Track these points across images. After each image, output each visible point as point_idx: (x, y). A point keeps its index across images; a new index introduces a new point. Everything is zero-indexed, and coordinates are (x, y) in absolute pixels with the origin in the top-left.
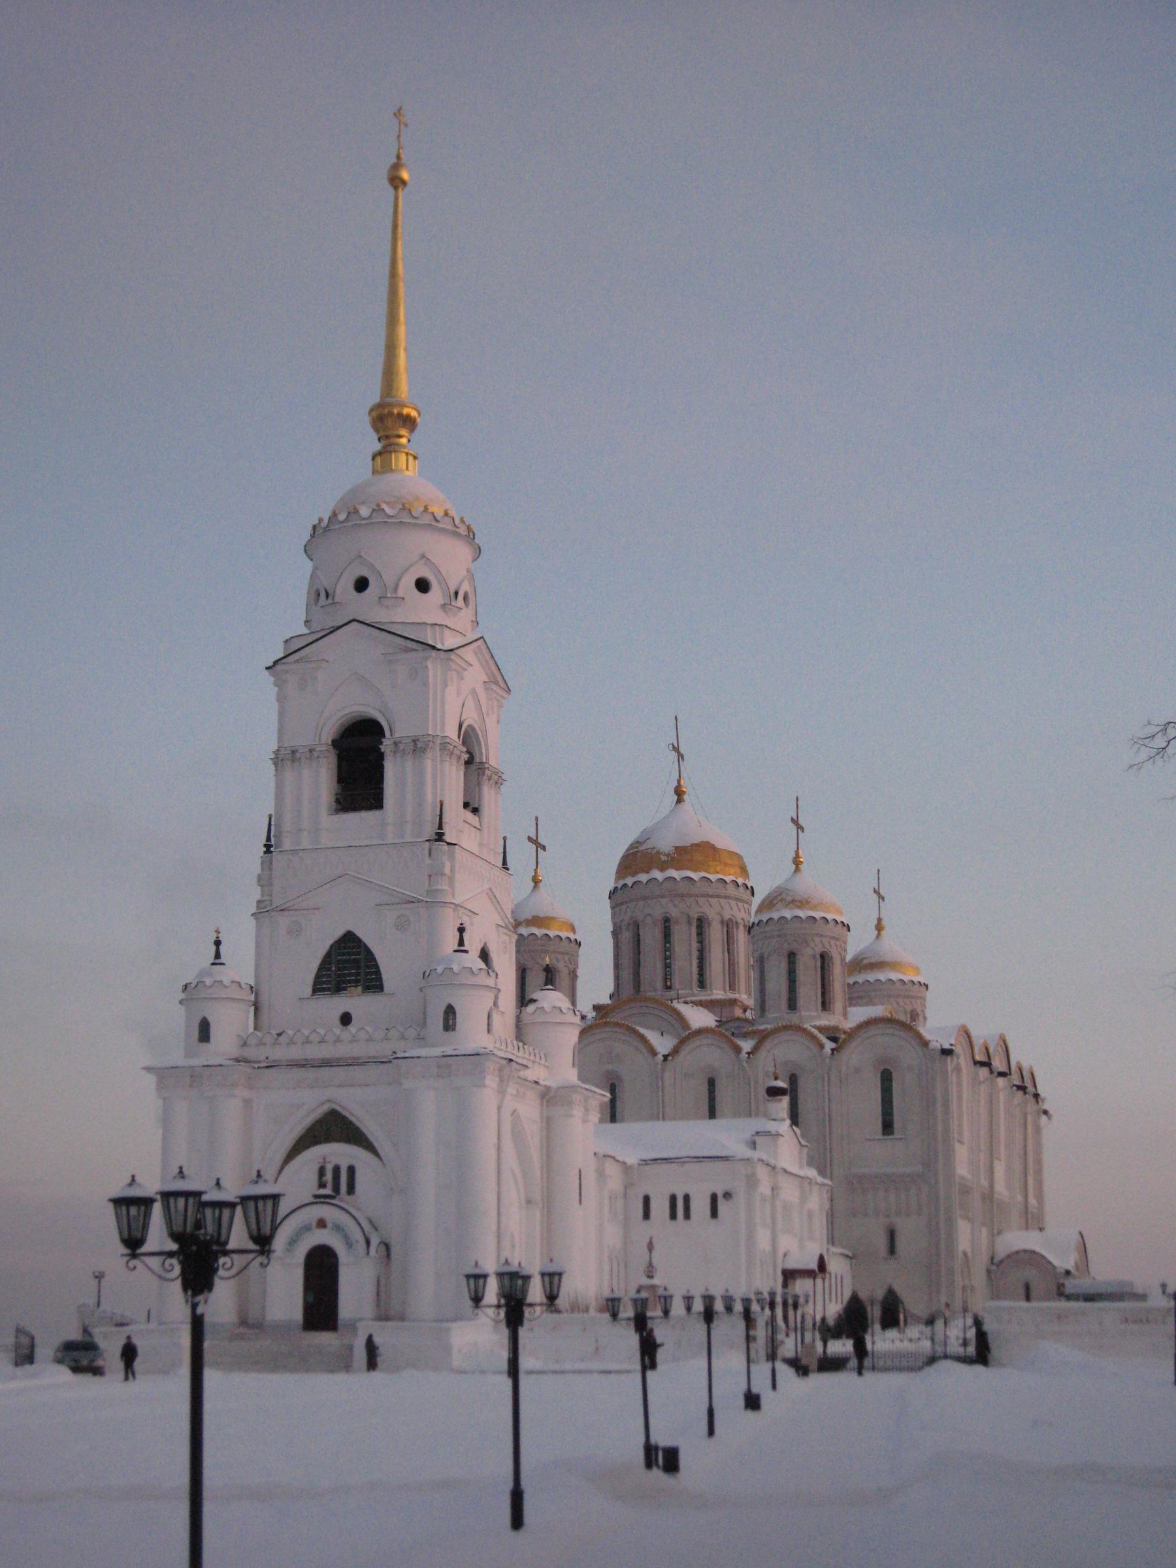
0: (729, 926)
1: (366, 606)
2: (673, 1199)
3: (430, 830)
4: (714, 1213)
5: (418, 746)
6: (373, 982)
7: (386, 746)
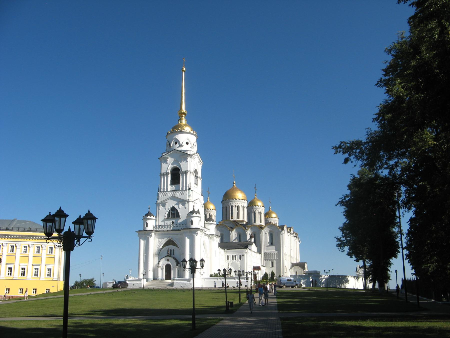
0: (243, 207)
2: (233, 256)
4: (240, 259)
5: (186, 172)
6: (178, 216)
7: (180, 172)
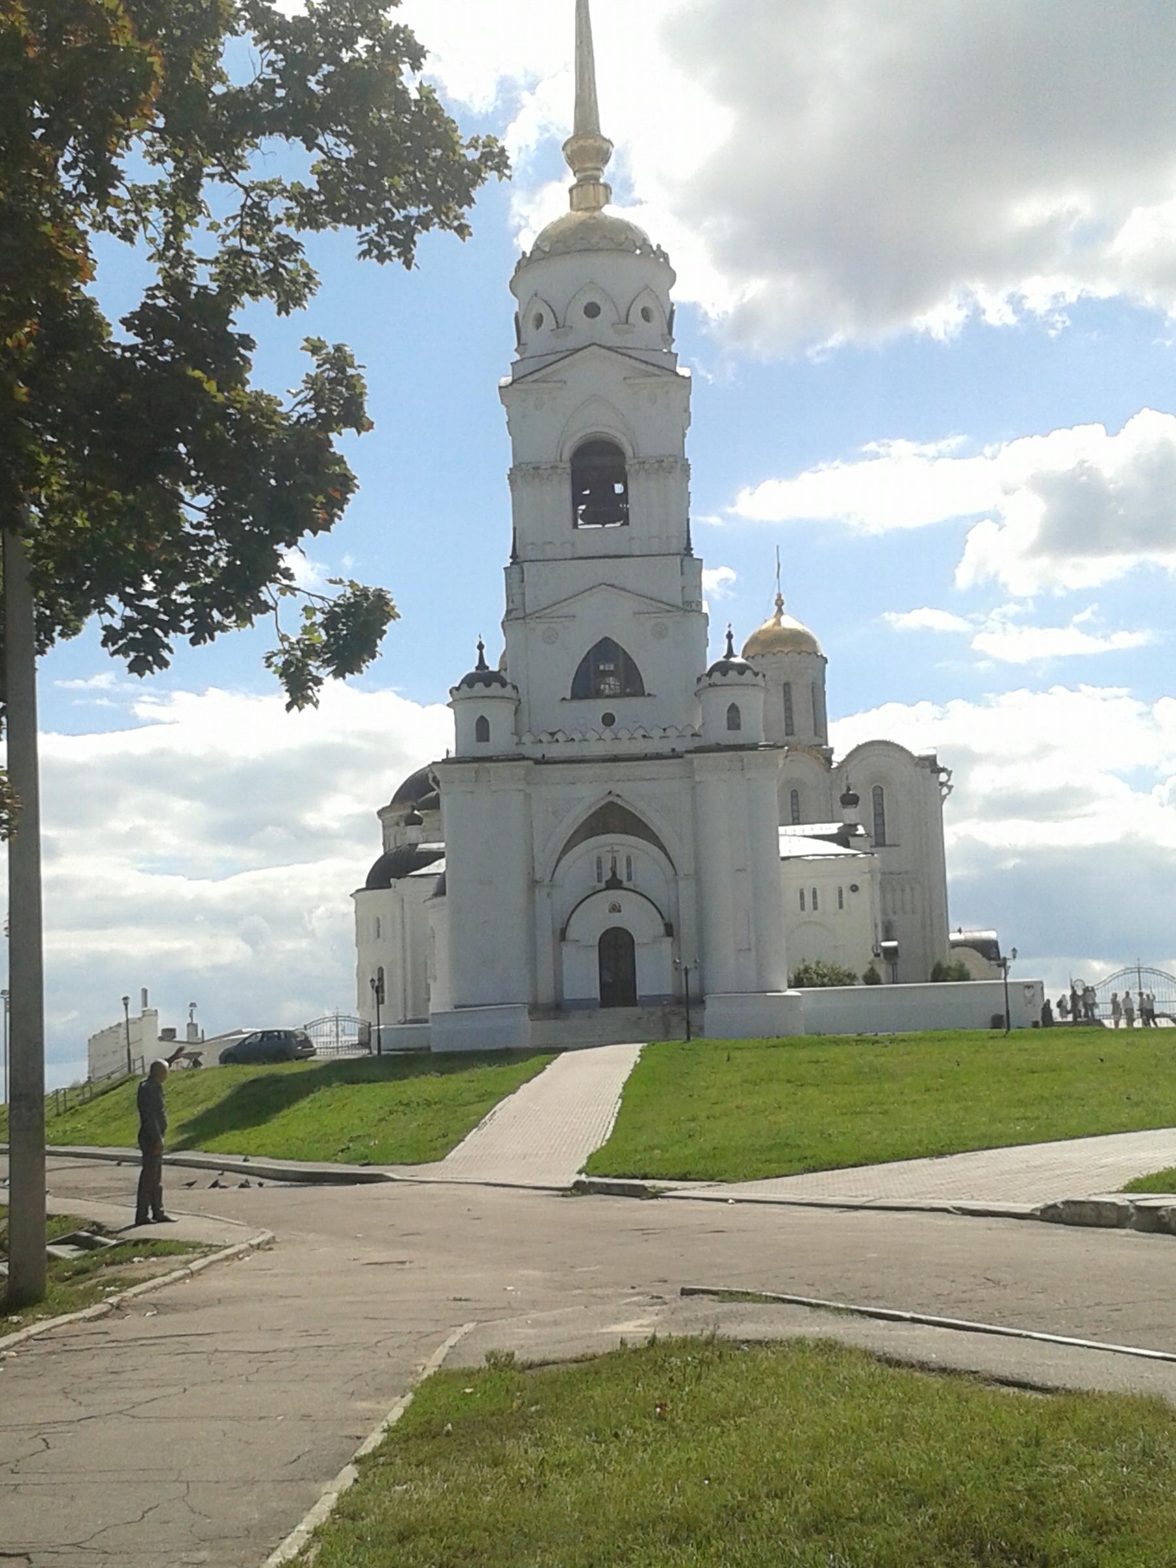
1: (602, 327)
3: (677, 546)
6: (632, 684)
